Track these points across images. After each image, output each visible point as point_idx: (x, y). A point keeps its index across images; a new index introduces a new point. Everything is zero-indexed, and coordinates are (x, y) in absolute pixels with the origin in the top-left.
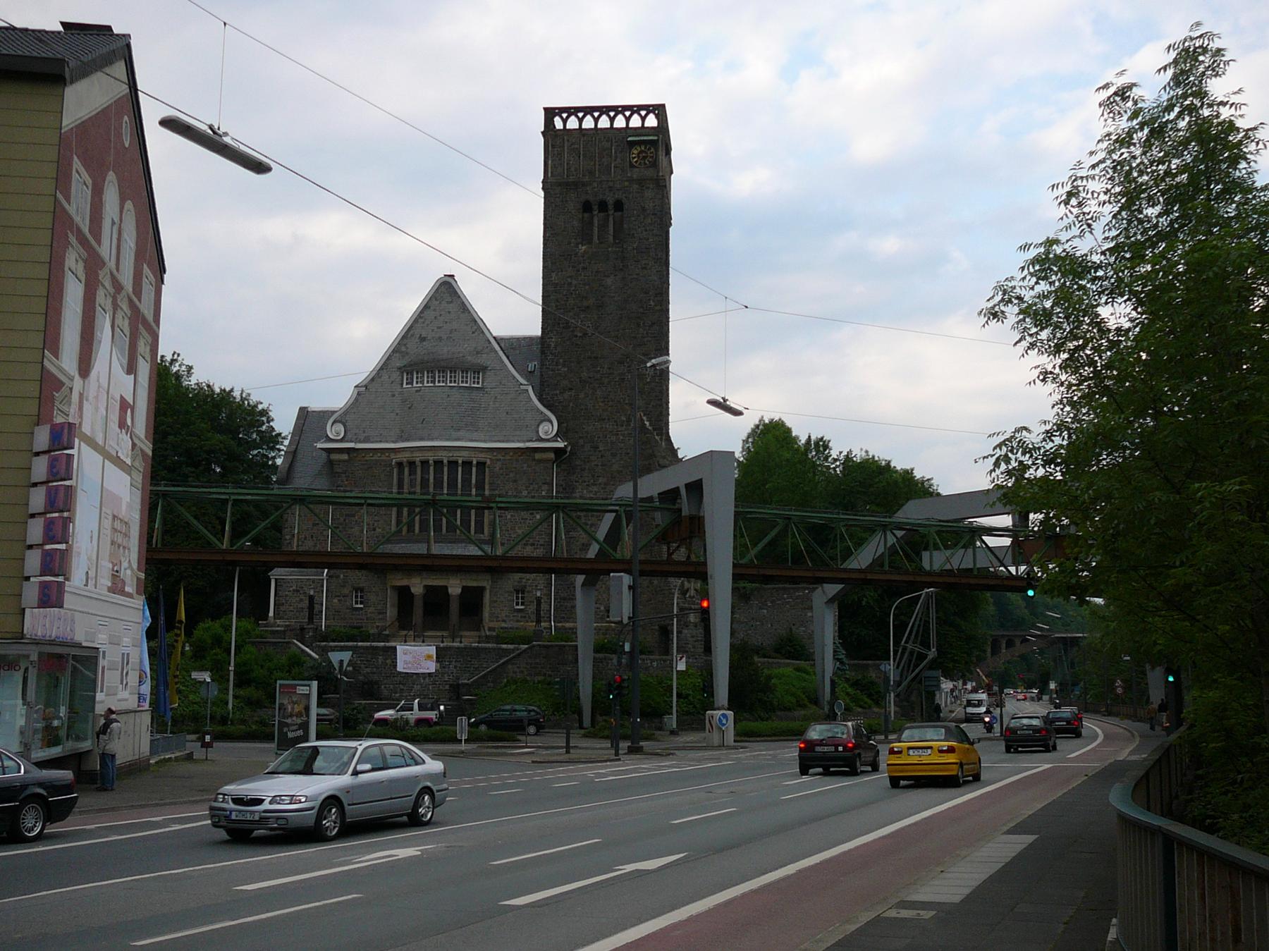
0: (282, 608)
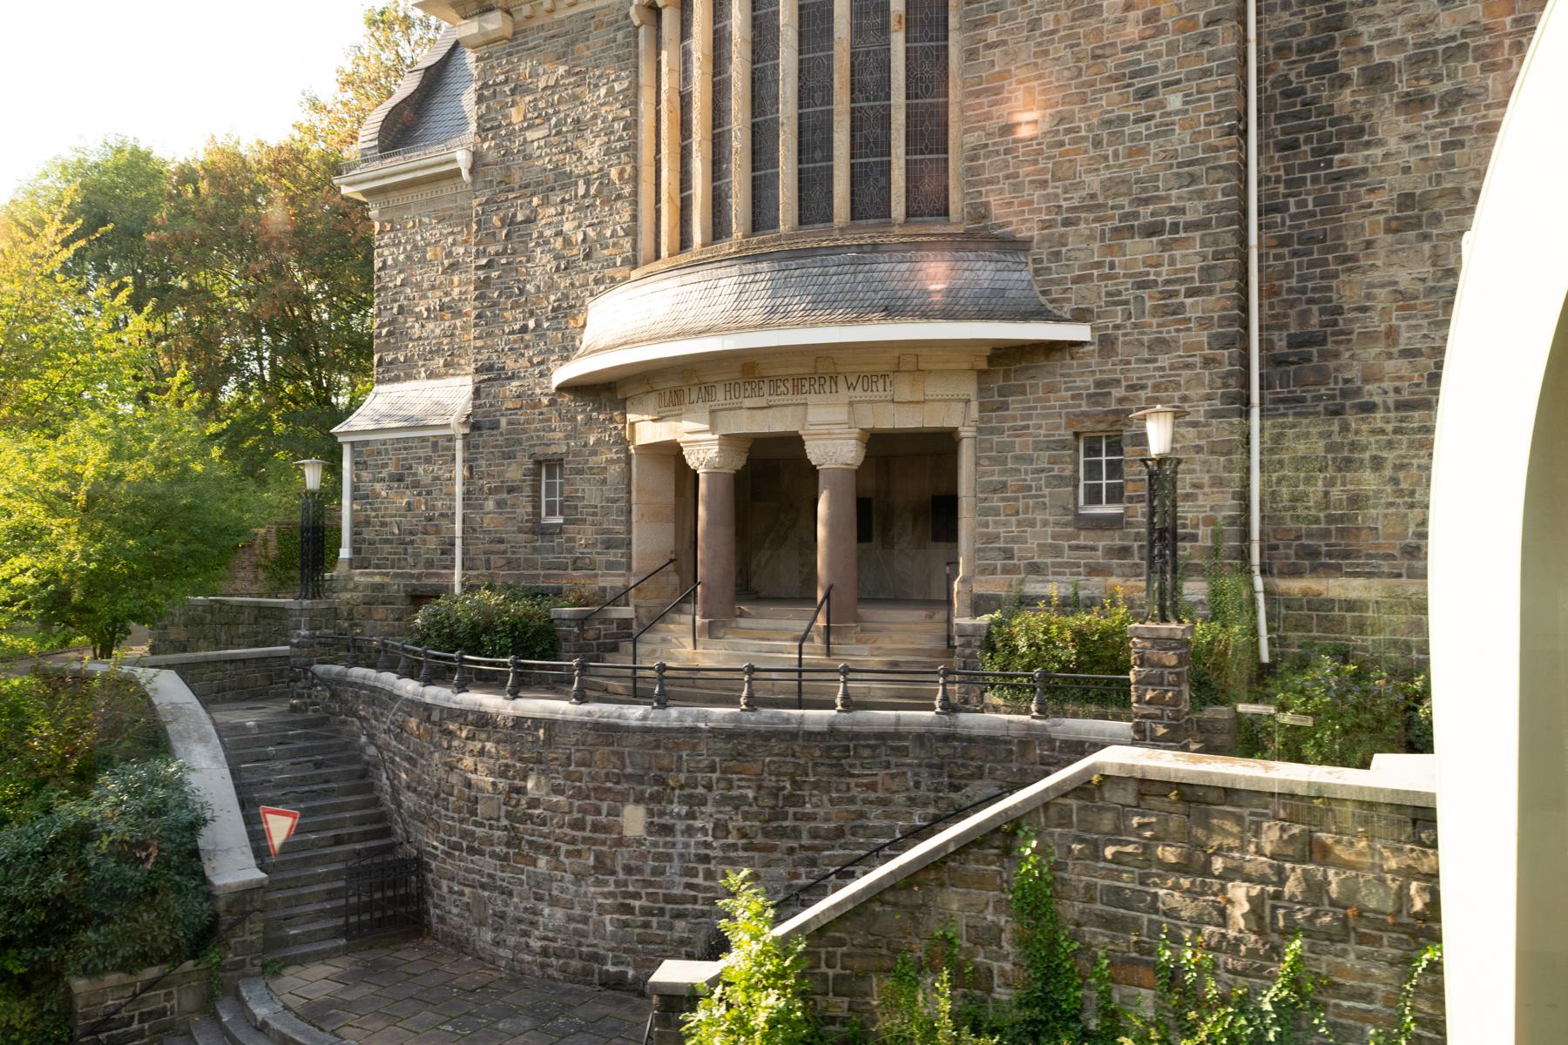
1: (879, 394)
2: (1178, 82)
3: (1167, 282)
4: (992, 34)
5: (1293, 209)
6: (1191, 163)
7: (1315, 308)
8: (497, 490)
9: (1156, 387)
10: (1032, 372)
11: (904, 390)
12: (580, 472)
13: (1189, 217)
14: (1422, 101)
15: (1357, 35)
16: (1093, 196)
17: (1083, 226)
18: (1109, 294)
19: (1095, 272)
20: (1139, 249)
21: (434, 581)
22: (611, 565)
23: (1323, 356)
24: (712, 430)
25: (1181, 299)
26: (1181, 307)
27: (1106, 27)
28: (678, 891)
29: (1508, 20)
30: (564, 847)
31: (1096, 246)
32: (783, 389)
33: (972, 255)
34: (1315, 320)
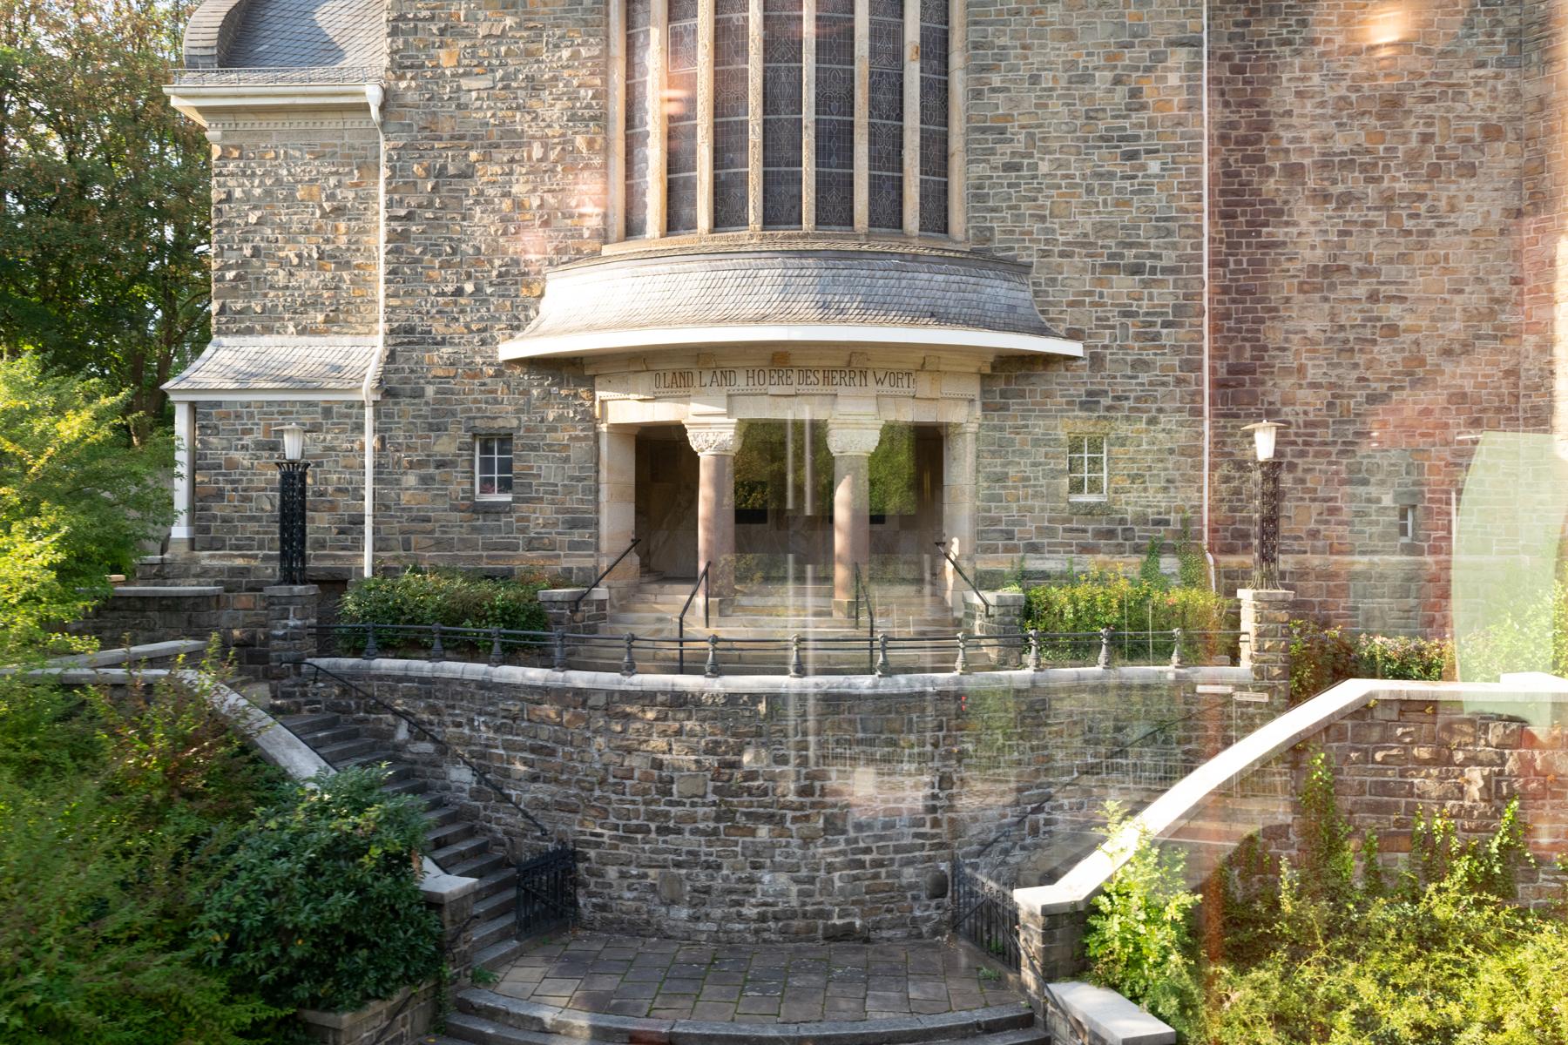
0: (217, 509)
1: (904, 389)
2: (1157, 151)
3: (1147, 314)
4: (996, 80)
5: (1232, 266)
6: (1166, 219)
7: (1248, 345)
8: (421, 464)
9: (1138, 399)
10: (1033, 379)
11: (924, 387)
12: (534, 448)
13: (1164, 263)
14: (1325, 196)
15: (1279, 138)
16: (1086, 235)
17: (1076, 259)
18: (1098, 319)
19: (1087, 299)
20: (1123, 284)
21: (328, 564)
22: (574, 546)
23: (1255, 383)
24: (729, 414)
25: (1158, 328)
26: (1156, 337)
27: (1099, 94)
28: (907, 841)
29: (1381, 147)
30: (790, 814)
31: (1088, 277)
32: (813, 379)
33: (991, 274)
34: (1248, 354)
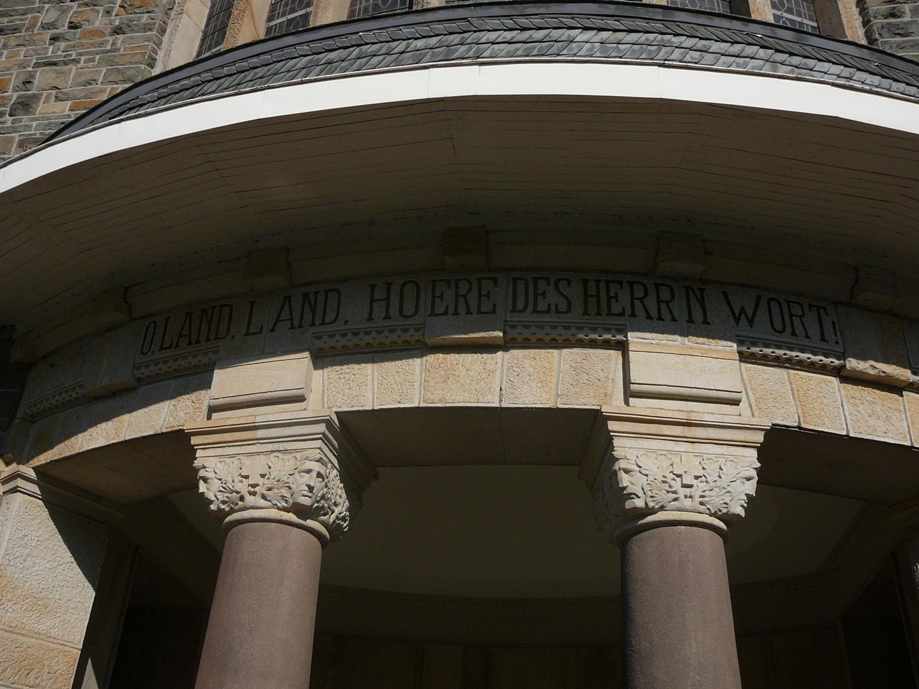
32: (553, 298)
